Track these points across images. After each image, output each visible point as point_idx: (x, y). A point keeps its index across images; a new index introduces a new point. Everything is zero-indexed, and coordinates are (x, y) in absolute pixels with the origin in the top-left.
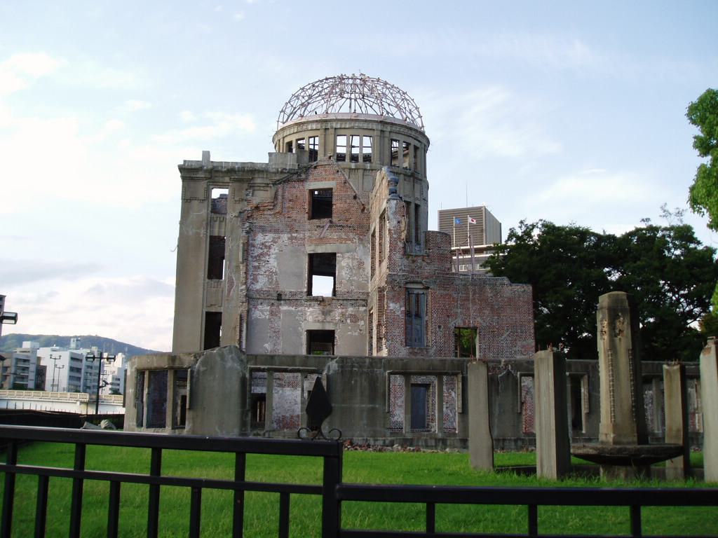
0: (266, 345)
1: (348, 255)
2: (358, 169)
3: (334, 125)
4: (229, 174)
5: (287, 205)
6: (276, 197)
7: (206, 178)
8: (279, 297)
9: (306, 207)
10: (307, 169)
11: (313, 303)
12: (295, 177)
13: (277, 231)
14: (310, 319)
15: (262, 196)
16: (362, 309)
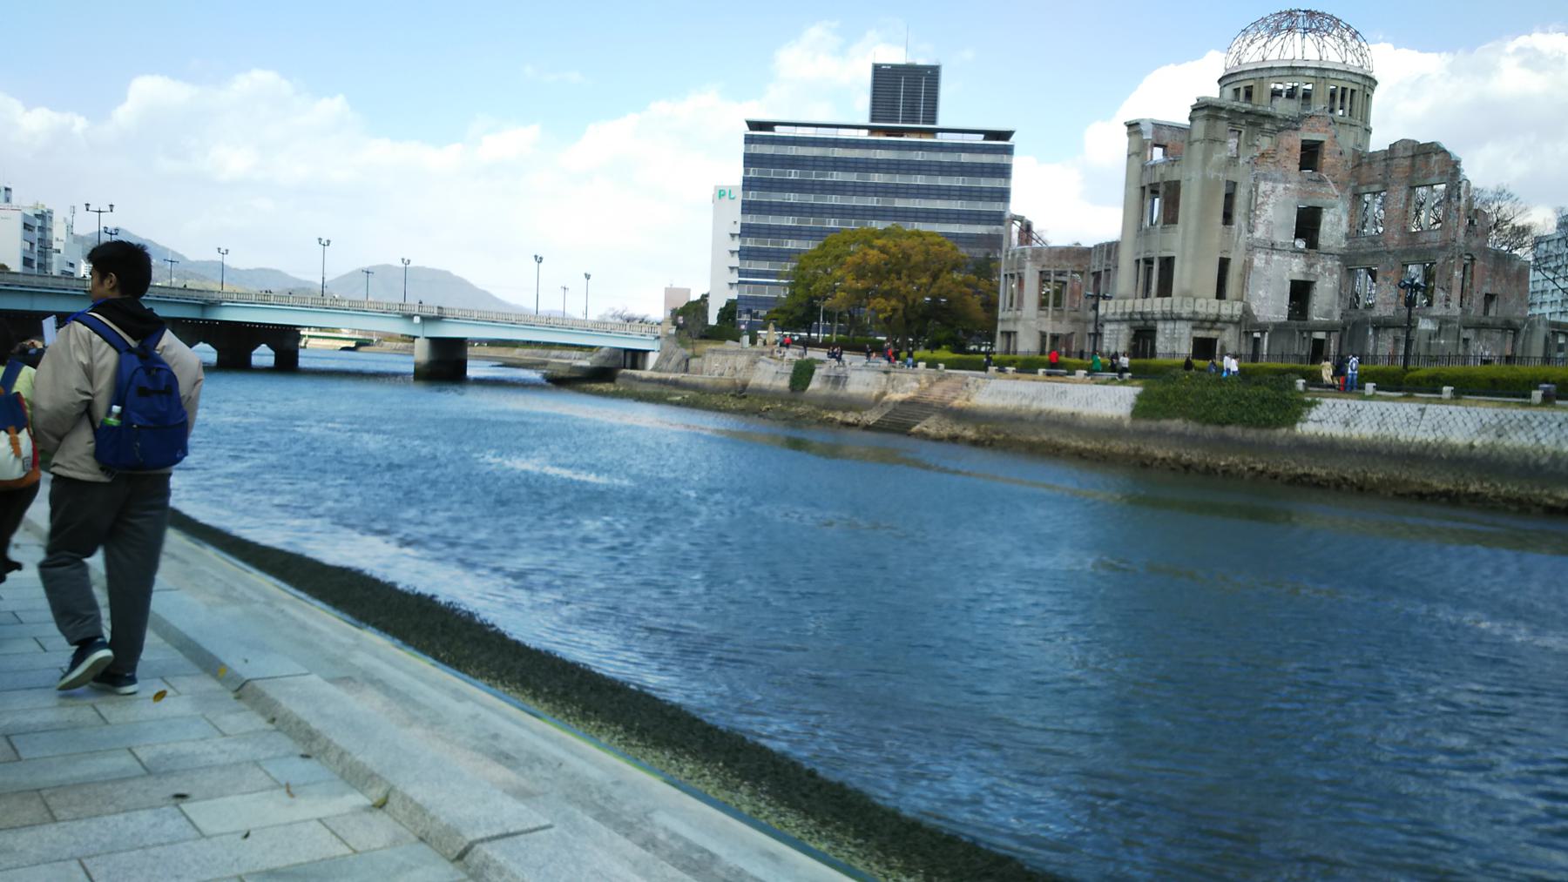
0: (1261, 292)
1: (1332, 210)
2: (1345, 124)
3: (1332, 75)
4: (1246, 116)
5: (1284, 154)
6: (1278, 146)
7: (1229, 119)
8: (1273, 247)
9: (1298, 157)
10: (1303, 117)
11: (1298, 255)
12: (1294, 125)
13: (1275, 181)
14: (1295, 269)
15: (1265, 143)
16: (1337, 263)
